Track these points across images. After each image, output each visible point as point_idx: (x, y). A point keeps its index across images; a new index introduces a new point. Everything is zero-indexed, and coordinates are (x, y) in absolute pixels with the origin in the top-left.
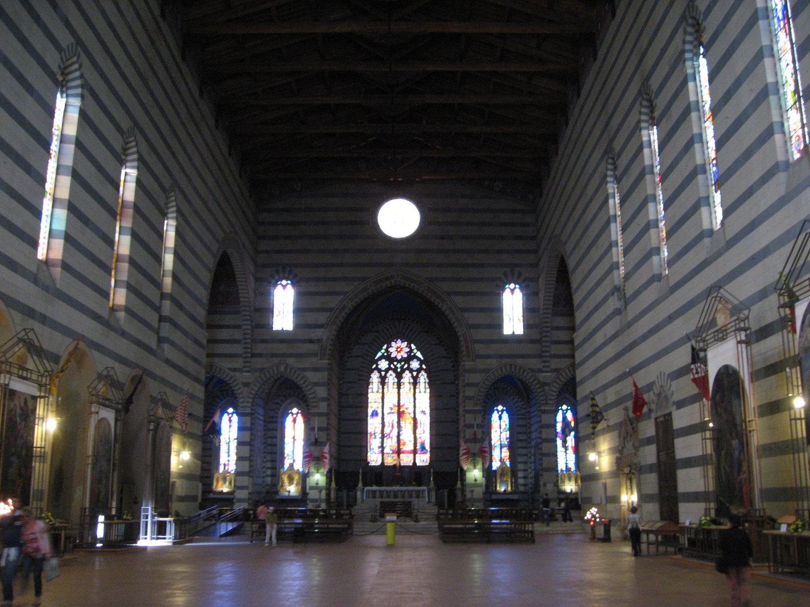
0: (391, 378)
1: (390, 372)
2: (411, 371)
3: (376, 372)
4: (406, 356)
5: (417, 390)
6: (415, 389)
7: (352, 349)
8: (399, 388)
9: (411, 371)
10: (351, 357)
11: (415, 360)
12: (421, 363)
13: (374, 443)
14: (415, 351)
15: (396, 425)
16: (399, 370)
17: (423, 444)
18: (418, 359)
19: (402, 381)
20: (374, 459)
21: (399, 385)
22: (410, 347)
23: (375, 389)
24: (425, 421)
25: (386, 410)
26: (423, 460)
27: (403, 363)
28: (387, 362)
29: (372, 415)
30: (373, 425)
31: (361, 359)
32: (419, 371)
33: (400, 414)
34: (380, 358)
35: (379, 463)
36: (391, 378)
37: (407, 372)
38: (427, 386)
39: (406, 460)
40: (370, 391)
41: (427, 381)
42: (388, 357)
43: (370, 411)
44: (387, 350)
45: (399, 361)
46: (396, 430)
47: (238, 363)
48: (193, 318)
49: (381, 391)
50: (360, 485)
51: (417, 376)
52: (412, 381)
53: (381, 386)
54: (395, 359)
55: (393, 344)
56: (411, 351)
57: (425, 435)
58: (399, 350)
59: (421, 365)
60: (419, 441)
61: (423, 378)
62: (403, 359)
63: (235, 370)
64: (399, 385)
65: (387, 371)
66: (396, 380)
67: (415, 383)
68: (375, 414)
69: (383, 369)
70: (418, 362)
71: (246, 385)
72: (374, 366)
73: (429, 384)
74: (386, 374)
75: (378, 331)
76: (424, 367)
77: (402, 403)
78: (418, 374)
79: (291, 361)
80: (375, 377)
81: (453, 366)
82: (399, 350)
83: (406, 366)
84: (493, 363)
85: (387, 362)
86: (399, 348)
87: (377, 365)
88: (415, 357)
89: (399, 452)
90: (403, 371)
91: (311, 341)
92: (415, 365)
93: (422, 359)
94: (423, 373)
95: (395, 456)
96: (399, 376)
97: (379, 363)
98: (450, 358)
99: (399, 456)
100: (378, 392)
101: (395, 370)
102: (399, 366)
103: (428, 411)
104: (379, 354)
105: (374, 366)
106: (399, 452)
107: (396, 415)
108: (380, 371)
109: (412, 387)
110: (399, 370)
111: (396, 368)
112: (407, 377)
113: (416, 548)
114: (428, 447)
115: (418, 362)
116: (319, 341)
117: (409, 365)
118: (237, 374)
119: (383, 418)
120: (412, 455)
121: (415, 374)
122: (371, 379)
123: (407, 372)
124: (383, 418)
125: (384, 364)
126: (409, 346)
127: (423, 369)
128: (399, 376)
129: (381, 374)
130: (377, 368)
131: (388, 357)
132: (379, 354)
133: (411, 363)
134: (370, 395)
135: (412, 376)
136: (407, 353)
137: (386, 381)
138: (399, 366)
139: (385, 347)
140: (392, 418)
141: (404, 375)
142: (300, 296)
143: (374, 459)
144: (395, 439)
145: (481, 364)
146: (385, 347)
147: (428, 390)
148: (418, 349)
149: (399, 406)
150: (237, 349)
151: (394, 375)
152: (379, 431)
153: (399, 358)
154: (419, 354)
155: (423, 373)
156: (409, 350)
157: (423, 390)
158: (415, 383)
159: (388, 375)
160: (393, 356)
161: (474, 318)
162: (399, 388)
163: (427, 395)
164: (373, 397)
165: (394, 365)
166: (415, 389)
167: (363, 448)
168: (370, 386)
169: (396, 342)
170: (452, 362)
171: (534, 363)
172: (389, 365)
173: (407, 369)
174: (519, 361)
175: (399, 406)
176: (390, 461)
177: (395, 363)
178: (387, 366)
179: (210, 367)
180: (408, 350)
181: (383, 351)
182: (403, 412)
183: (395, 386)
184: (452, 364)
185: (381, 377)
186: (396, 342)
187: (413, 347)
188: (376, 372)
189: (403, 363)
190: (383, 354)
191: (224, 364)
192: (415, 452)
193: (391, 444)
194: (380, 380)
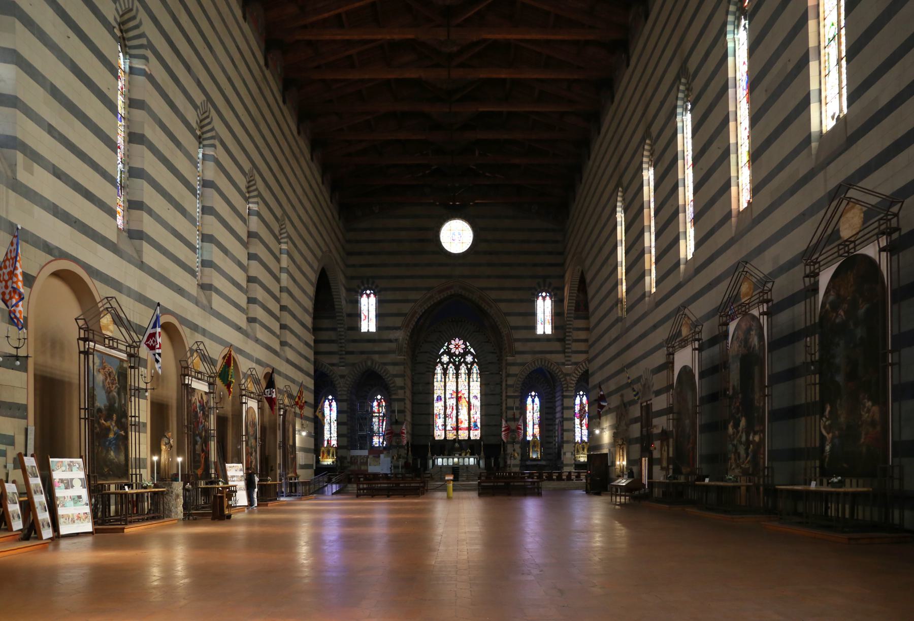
0: (451, 370)
2: (466, 364)
3: (439, 365)
6: (469, 378)
7: (421, 346)
8: (457, 378)
9: (466, 364)
11: (469, 355)
12: (474, 357)
13: (439, 422)
14: (469, 347)
15: (455, 408)
16: (457, 363)
17: (475, 422)
18: (472, 354)
19: (460, 372)
20: (439, 434)
21: (457, 375)
22: (466, 345)
23: (439, 379)
24: (476, 403)
25: (448, 396)
26: (476, 435)
28: (448, 357)
29: (437, 400)
30: (438, 407)
32: (472, 364)
33: (458, 399)
34: (443, 354)
35: (443, 438)
36: (451, 370)
37: (463, 365)
38: (479, 376)
39: (463, 435)
40: (435, 380)
41: (479, 372)
42: (448, 353)
43: (435, 397)
44: (448, 347)
45: (457, 356)
46: (455, 411)
47: (335, 359)
48: (303, 325)
49: (443, 380)
50: (429, 455)
51: (471, 368)
52: (467, 372)
53: (443, 377)
54: (454, 354)
55: (453, 342)
57: (477, 415)
58: (457, 346)
60: (472, 420)
61: (475, 369)
62: (460, 354)
63: (333, 365)
64: (457, 375)
65: (448, 364)
66: (455, 372)
67: (469, 374)
68: (439, 398)
69: (445, 362)
71: (342, 377)
72: (438, 360)
73: (480, 374)
74: (447, 367)
77: (459, 390)
78: (471, 367)
79: (376, 357)
80: (439, 369)
81: (498, 360)
82: (457, 346)
83: (462, 360)
84: (528, 358)
85: (448, 357)
86: (457, 345)
87: (441, 359)
89: (457, 429)
90: (460, 364)
91: (390, 341)
92: (469, 359)
94: (475, 365)
95: (455, 432)
96: (457, 368)
97: (442, 357)
98: (496, 353)
99: (457, 432)
100: (441, 381)
101: (454, 364)
102: (457, 359)
103: (479, 396)
104: (442, 350)
105: (438, 360)
106: (457, 429)
108: (442, 364)
110: (457, 363)
112: (463, 369)
113: (469, 498)
115: (472, 357)
116: (396, 340)
117: (465, 359)
118: (335, 368)
119: (445, 402)
120: (467, 432)
121: (469, 366)
122: (436, 372)
123: (463, 365)
124: (445, 402)
125: (445, 359)
126: (464, 343)
127: (475, 362)
128: (457, 368)
131: (448, 353)
132: (442, 350)
133: (466, 357)
134: (435, 384)
135: (467, 368)
136: (463, 349)
139: (446, 344)
140: (451, 402)
141: (461, 367)
142: (379, 303)
143: (439, 434)
144: (454, 419)
145: (519, 359)
146: (446, 344)
147: (479, 380)
149: (457, 392)
150: (333, 347)
151: (453, 367)
152: (442, 412)
154: (472, 350)
155: (475, 365)
157: (475, 379)
158: (469, 374)
159: (449, 367)
161: (514, 321)
162: (457, 378)
163: (479, 384)
164: (438, 385)
166: (469, 378)
167: (431, 426)
168: (436, 376)
169: (455, 340)
171: (559, 358)
172: (450, 359)
173: (463, 362)
174: (548, 356)
175: (457, 392)
176: (451, 436)
178: (448, 360)
179: (316, 363)
181: (445, 348)
182: (461, 397)
186: (455, 340)
187: (468, 344)
188: (439, 365)
190: (445, 350)
191: (326, 360)
192: (469, 429)
193: (451, 423)
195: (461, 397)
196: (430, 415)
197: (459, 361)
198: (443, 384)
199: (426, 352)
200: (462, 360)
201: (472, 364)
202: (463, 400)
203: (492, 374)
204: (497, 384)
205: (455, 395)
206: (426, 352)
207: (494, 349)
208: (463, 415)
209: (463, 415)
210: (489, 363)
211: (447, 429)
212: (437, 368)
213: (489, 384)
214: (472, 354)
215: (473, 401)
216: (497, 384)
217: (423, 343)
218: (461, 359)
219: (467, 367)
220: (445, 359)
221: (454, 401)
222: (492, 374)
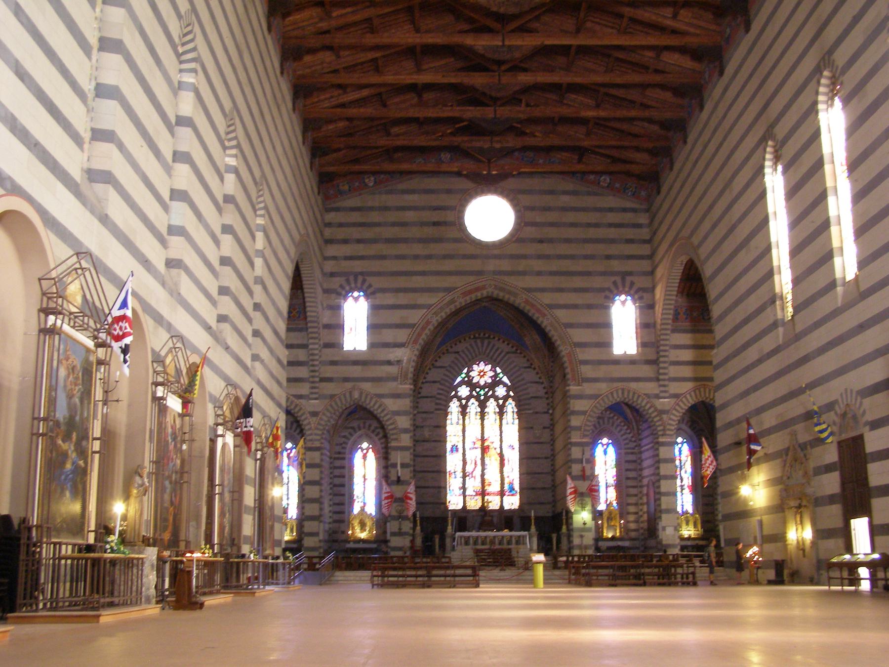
0: (473, 407)
1: (473, 400)
2: (497, 399)
3: (455, 400)
4: (490, 381)
5: (504, 421)
6: (501, 419)
8: (482, 419)
9: (497, 399)
10: (426, 382)
11: (501, 386)
12: (509, 389)
13: (454, 484)
14: (501, 375)
16: (482, 398)
17: (511, 484)
18: (505, 385)
19: (486, 410)
22: (495, 371)
23: (455, 420)
24: (513, 458)
26: (512, 502)
27: (486, 390)
28: (468, 389)
29: (452, 451)
30: (453, 462)
31: (438, 385)
32: (506, 398)
33: (485, 450)
34: (460, 384)
37: (492, 400)
38: (516, 416)
39: (494, 503)
40: (448, 422)
41: (516, 410)
42: (469, 383)
43: (449, 447)
49: (461, 422)
52: (497, 410)
53: (461, 417)
54: (477, 385)
55: (475, 367)
56: (496, 375)
58: (482, 374)
59: (508, 391)
60: (507, 481)
61: (511, 406)
63: (300, 397)
65: (468, 398)
66: (479, 410)
67: (501, 413)
68: (455, 449)
69: (464, 396)
70: (505, 389)
71: (314, 414)
74: (467, 403)
75: (456, 353)
76: (511, 394)
77: (486, 437)
78: (504, 403)
80: (454, 406)
81: (546, 393)
82: (482, 374)
83: (491, 393)
85: (468, 389)
86: (482, 372)
87: (457, 392)
88: (500, 382)
89: (483, 493)
90: (487, 399)
92: (501, 391)
93: (510, 384)
94: (510, 400)
96: (483, 405)
97: (459, 389)
98: (542, 383)
100: (458, 423)
101: (477, 398)
102: (482, 392)
103: (517, 445)
104: (459, 379)
106: (483, 493)
107: (479, 451)
108: (460, 399)
109: (498, 417)
110: (482, 398)
111: (479, 395)
112: (492, 405)
114: (517, 487)
115: (505, 389)
117: (494, 392)
118: (303, 401)
119: (464, 454)
121: (501, 402)
122: (449, 410)
123: (492, 400)
124: (464, 454)
125: (464, 391)
126: (493, 369)
127: (510, 396)
128: (483, 405)
129: (461, 403)
130: (456, 396)
131: (469, 383)
132: (459, 379)
134: (449, 428)
135: (498, 405)
137: (468, 411)
138: (482, 392)
139: (465, 371)
140: (474, 455)
141: (488, 404)
144: (479, 479)
146: (465, 371)
147: (517, 421)
148: (505, 373)
149: (483, 440)
151: (477, 403)
153: (482, 383)
154: (505, 379)
155: (510, 400)
156: (493, 374)
158: (501, 413)
159: (470, 404)
160: (475, 381)
162: (482, 419)
163: (516, 427)
166: (501, 419)
169: (478, 365)
170: (544, 388)
172: (471, 391)
173: (491, 396)
175: (483, 440)
176: (474, 504)
177: (478, 390)
178: (468, 393)
180: (492, 374)
181: (463, 375)
182: (488, 447)
183: (479, 417)
184: (545, 391)
185: (461, 406)
186: (478, 365)
187: (498, 370)
188: (455, 400)
189: (486, 390)
192: (502, 493)
193: (473, 485)
194: (460, 410)
195: (488, 447)
196: (440, 472)
199: (434, 382)
200: (491, 393)
201: (506, 398)
203: (537, 413)
204: (544, 428)
205: (479, 444)
206: (434, 382)
207: (540, 378)
208: (493, 475)
209: (493, 475)
210: (532, 397)
211: (467, 493)
212: (451, 404)
213: (532, 428)
214: (505, 385)
215: (507, 453)
216: (544, 428)
217: (430, 369)
220: (464, 391)
221: (478, 452)
222: (537, 413)
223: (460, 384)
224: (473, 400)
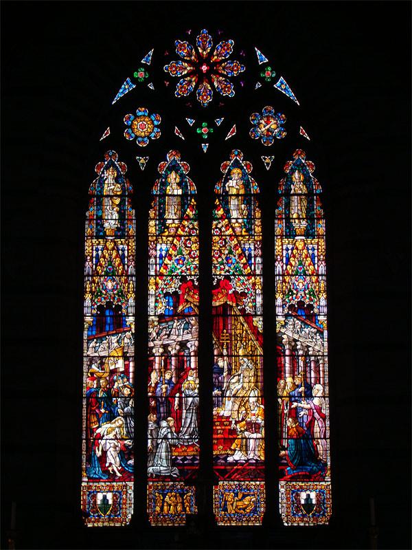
2: (253, 150)
3: (112, 156)
9: (253, 150)
17: (305, 436)
18: (281, 103)
25: (156, 307)
32: (283, 150)
34: (130, 104)
38: (318, 209)
44: (155, 72)
45: (205, 115)
46: (192, 380)
49: (132, 229)
52: (255, 188)
54: (190, 105)
59: (290, 127)
65: (156, 150)
66: (193, 189)
68: (109, 321)
72: (107, 133)
74: (152, 166)
82: (203, 70)
87: (119, 128)
90: (221, 150)
92: (268, 126)
100: (120, 233)
101: (189, 149)
102: (204, 131)
104: (126, 88)
105: (107, 133)
108: (128, 151)
111: (194, 139)
117: (245, 127)
119: (141, 337)
120: (257, 485)
122: (93, 188)
124: (141, 337)
125: (143, 127)
129: (133, 165)
132: (126, 88)
135: (259, 172)
139: (147, 60)
144: (189, 420)
149: (206, 284)
152: (123, 386)
154: (282, 85)
159: (163, 166)
160: (179, 92)
163: (319, 246)
165: (184, 128)
169: (192, 42)
172: (165, 127)
173: (234, 143)
175: (206, 284)
180: (239, 69)
186: (192, 42)
188: (112, 156)
190: (141, 86)
192: (270, 470)
197: (217, 136)
198: (128, 247)
202: (239, 327)
214: (281, 103)
215: (289, 331)
218: (225, 128)
219: (258, 166)
220: (143, 127)
223: (130, 104)
224: (172, 157)
